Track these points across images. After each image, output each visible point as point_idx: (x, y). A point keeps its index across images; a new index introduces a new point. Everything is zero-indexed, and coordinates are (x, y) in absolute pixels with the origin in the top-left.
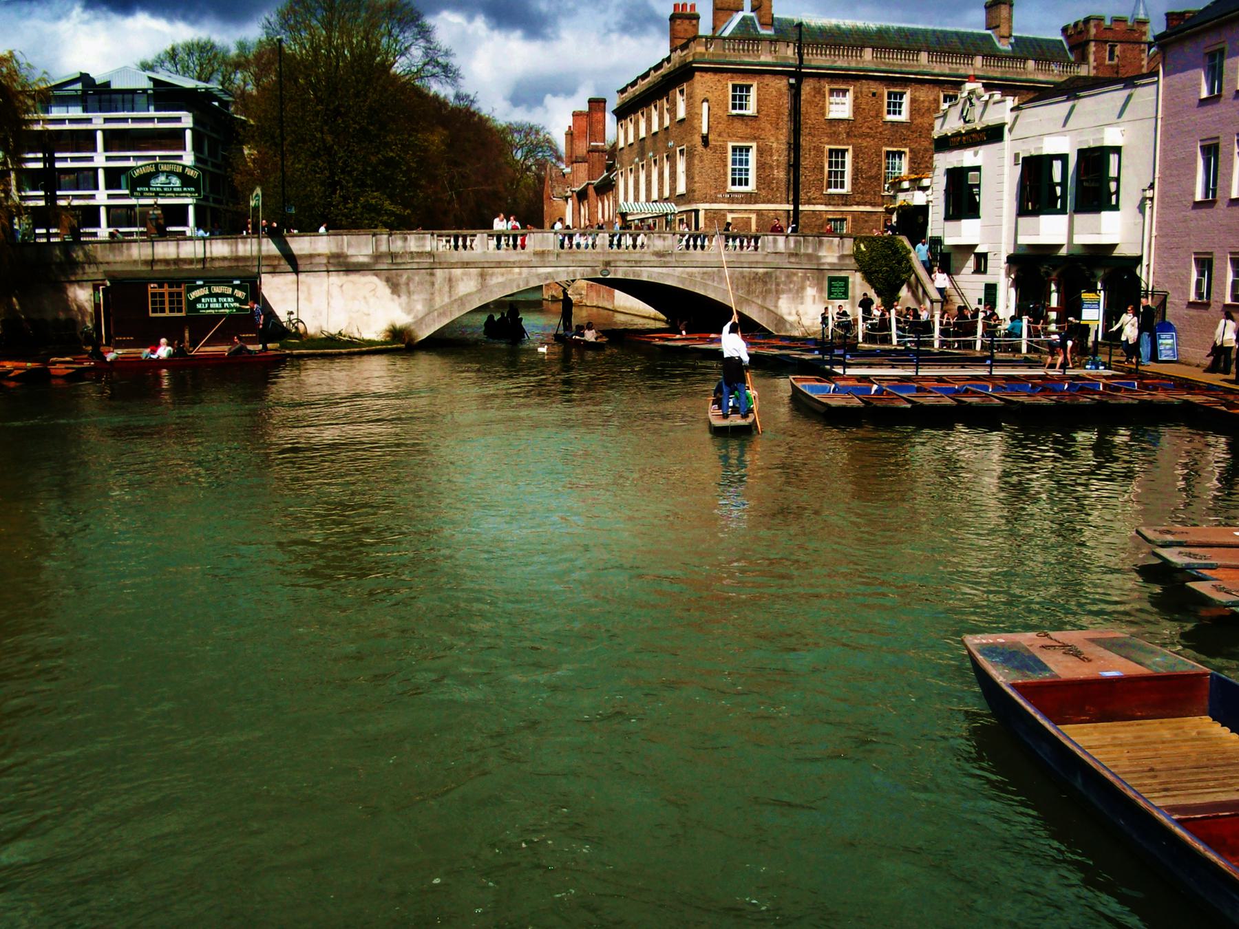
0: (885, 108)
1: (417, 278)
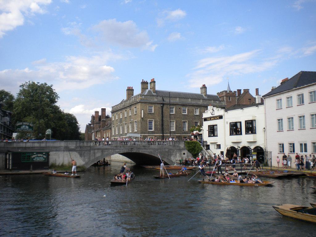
0: (182, 111)
1: (86, 153)
